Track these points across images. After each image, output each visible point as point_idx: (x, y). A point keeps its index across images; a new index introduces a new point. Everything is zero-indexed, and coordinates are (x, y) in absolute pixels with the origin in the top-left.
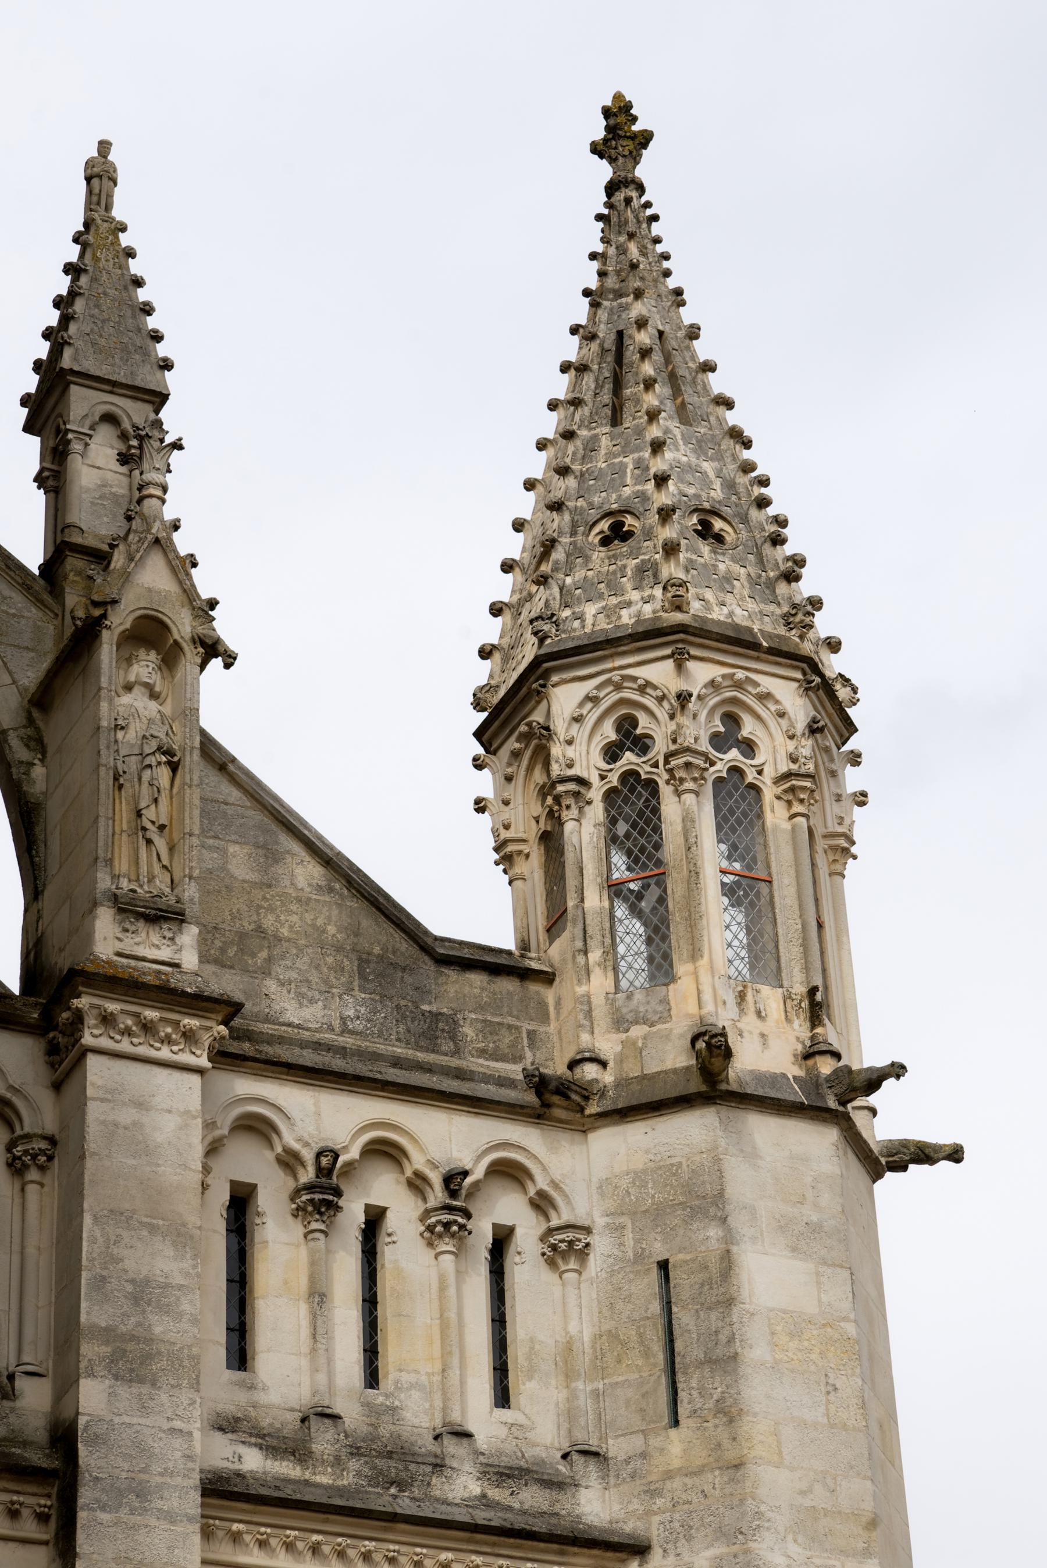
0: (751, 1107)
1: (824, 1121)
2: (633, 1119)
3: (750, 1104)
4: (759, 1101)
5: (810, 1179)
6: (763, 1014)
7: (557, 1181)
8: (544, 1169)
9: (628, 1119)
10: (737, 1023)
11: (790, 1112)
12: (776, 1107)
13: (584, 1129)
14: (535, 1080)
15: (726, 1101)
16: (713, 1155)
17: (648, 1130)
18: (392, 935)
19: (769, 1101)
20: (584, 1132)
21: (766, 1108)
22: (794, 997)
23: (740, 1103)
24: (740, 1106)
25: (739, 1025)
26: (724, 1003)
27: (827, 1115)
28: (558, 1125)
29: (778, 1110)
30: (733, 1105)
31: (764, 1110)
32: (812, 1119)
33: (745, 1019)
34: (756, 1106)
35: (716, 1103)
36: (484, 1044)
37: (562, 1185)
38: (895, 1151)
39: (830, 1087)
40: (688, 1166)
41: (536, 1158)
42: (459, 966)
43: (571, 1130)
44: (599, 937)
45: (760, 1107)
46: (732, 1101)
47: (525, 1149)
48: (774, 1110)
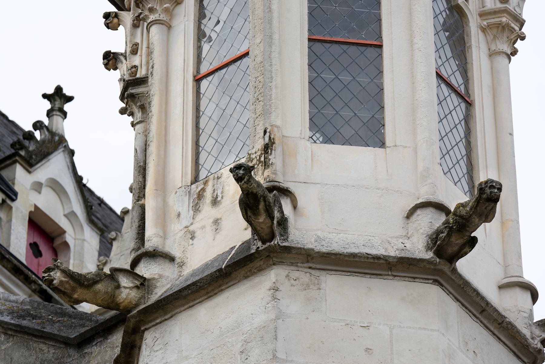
0: (178, 310)
1: (260, 270)
3: (176, 308)
4: (176, 299)
11: (220, 286)
12: (203, 292)
15: (151, 321)
18: (41, 350)
19: (186, 292)
21: (194, 300)
22: (253, 156)
23: (166, 314)
24: (166, 317)
25: (191, 228)
26: (179, 215)
27: (258, 263)
29: (207, 293)
30: (158, 321)
31: (191, 304)
32: (246, 277)
33: (200, 216)
34: (183, 305)
35: (143, 331)
38: (434, 237)
42: (101, 337)
45: (188, 303)
46: (157, 318)
48: (203, 296)
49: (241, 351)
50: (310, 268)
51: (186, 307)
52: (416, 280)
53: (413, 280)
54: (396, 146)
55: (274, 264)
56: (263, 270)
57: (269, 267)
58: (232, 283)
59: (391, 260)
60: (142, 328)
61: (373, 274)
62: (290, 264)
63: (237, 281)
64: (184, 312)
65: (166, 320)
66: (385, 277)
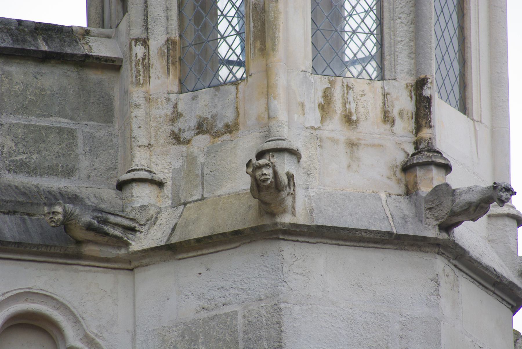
0: (325, 241)
2: (185, 255)
5: (398, 327)
6: (354, 118)
7: (93, 336)
8: (76, 321)
9: (180, 257)
10: (317, 132)
13: (130, 267)
14: (56, 218)
16: (273, 303)
17: (203, 270)
20: (132, 270)
28: (97, 264)
31: (341, 242)
36: (25, 156)
37: (98, 340)
39: (430, 209)
40: (244, 316)
41: (67, 308)
43: (115, 269)
44: (163, 20)
47: (52, 298)
49: (400, 334)
50: (455, 266)
51: (334, 242)
52: (504, 302)
53: (501, 300)
54: (481, 122)
55: (438, 254)
56: (425, 252)
57: (432, 253)
58: (389, 246)
59: (504, 281)
60: (281, 237)
61: (483, 286)
62: (447, 257)
63: (395, 248)
64: (329, 245)
65: (308, 242)
66: (489, 292)
